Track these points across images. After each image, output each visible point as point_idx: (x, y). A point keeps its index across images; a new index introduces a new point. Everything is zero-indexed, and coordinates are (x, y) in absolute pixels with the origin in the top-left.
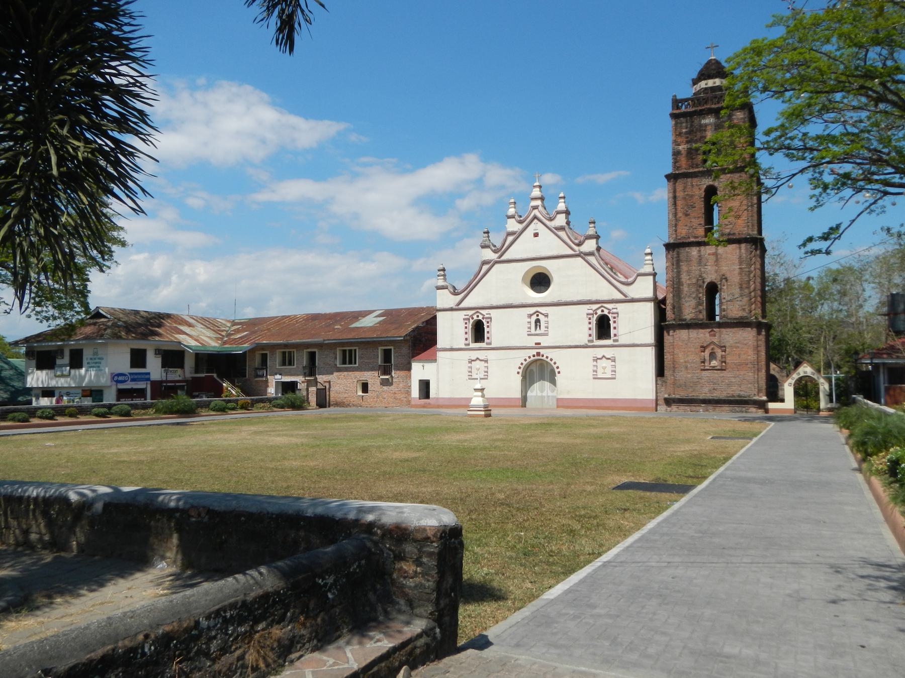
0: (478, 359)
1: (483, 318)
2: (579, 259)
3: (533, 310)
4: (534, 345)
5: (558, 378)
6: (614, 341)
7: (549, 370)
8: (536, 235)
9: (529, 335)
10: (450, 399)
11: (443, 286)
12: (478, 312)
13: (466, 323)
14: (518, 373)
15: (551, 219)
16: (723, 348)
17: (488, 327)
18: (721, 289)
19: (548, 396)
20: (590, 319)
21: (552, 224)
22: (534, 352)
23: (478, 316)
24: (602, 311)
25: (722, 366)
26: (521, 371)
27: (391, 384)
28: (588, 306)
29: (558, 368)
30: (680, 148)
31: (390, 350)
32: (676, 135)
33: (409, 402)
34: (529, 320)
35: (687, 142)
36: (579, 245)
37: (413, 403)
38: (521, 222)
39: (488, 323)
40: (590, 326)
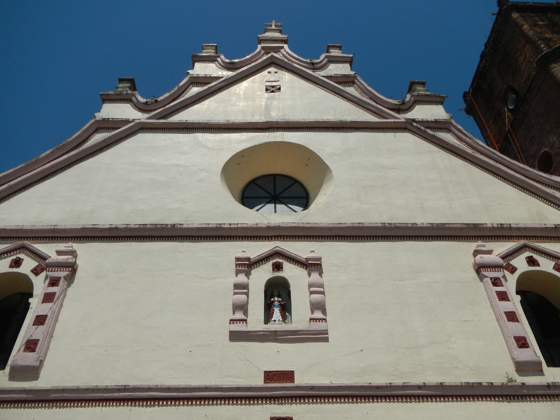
1: (36, 271)
4: (259, 382)
8: (273, 89)
9: (235, 336)
12: (23, 248)
15: (314, 67)
17: (48, 298)
20: (496, 282)
21: (319, 74)
23: (17, 263)
24: (531, 261)
28: (473, 246)
30: (547, 36)
32: (530, 26)
34: (242, 278)
35: (553, 33)
36: (399, 110)
38: (229, 67)
39: (54, 282)
40: (506, 306)
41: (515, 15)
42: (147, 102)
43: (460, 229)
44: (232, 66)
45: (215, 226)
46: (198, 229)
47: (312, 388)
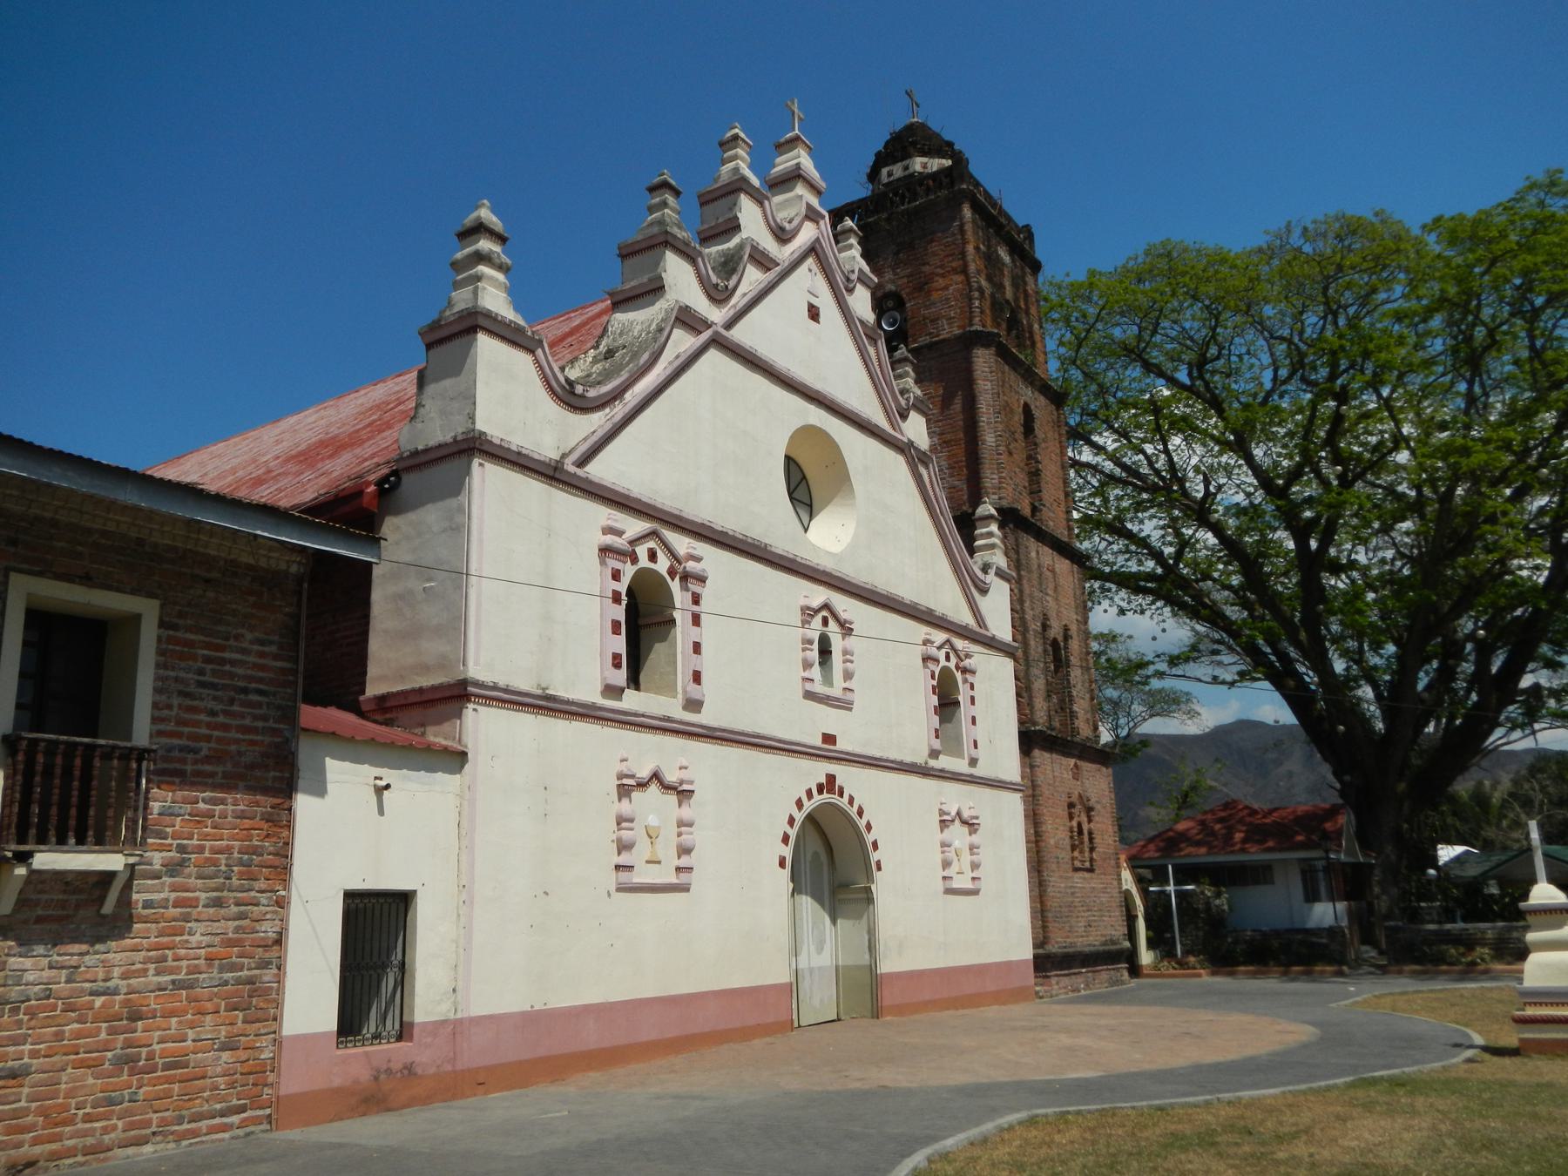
0: (656, 776)
2: (900, 459)
3: (818, 595)
4: (818, 742)
5: (882, 887)
6: (973, 762)
7: (809, 857)
10: (531, 1019)
11: (519, 330)
12: (653, 534)
13: (616, 576)
14: (782, 864)
16: (1089, 810)
18: (1068, 661)
19: (811, 970)
22: (818, 771)
23: (652, 556)
25: (1091, 860)
26: (787, 852)
27: (119, 924)
29: (875, 845)
31: (136, 619)
33: (258, 1074)
37: (292, 1081)
41: (967, 212)
42: (717, 285)
43: (923, 612)
44: (779, 233)
45: (791, 556)
46: (781, 557)
47: (847, 753)
